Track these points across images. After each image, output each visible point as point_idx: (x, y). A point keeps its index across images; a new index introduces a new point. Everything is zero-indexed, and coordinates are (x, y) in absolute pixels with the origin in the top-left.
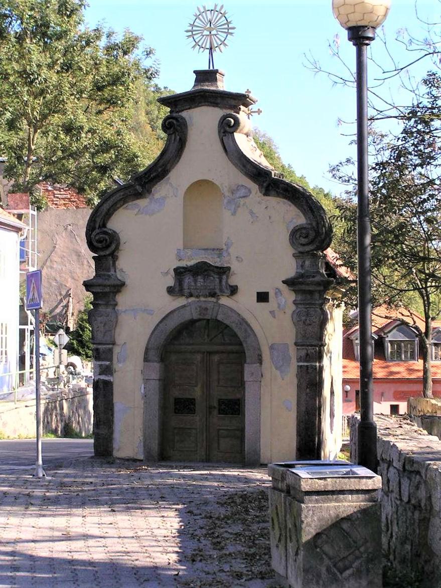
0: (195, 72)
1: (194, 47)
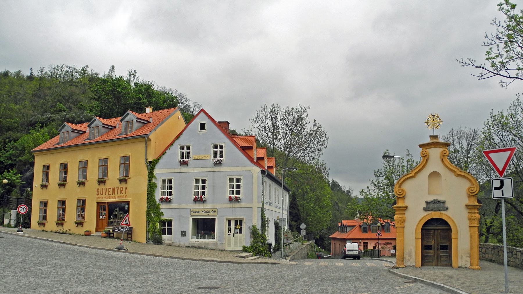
0: (430, 136)
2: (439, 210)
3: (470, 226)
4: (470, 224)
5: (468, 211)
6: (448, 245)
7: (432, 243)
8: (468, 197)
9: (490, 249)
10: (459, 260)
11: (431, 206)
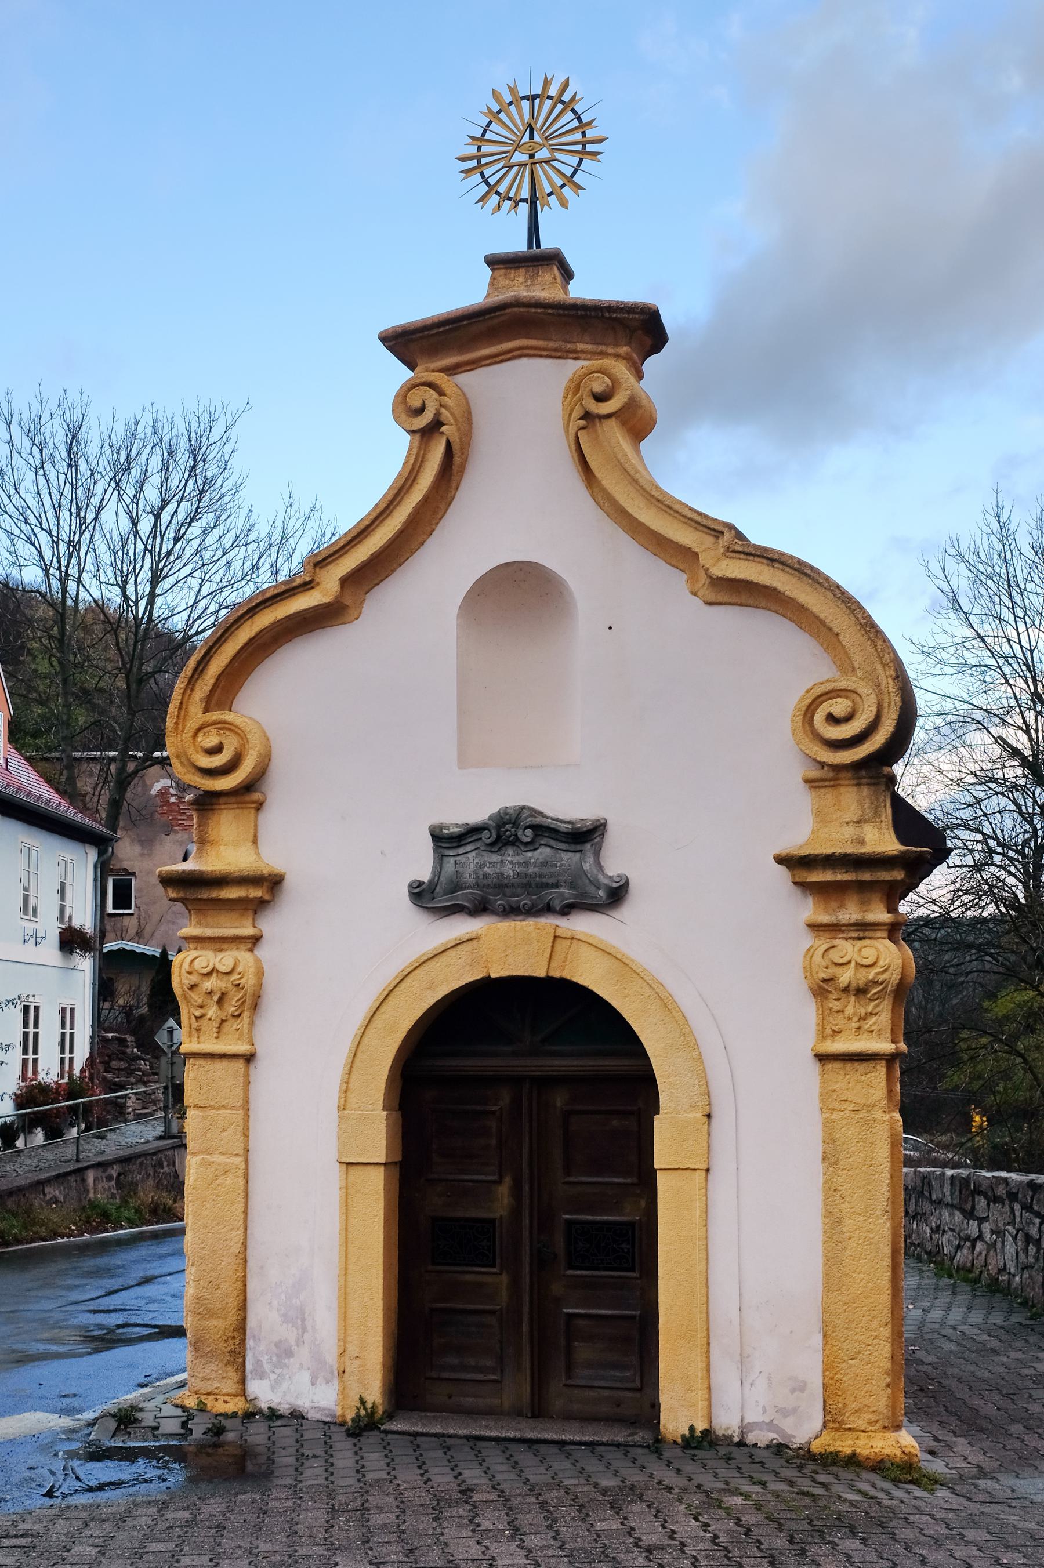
0: (494, 262)
1: (483, 199)
2: (548, 909)
3: (822, 1058)
5: (808, 909)
6: (631, 1224)
10: (725, 1374)
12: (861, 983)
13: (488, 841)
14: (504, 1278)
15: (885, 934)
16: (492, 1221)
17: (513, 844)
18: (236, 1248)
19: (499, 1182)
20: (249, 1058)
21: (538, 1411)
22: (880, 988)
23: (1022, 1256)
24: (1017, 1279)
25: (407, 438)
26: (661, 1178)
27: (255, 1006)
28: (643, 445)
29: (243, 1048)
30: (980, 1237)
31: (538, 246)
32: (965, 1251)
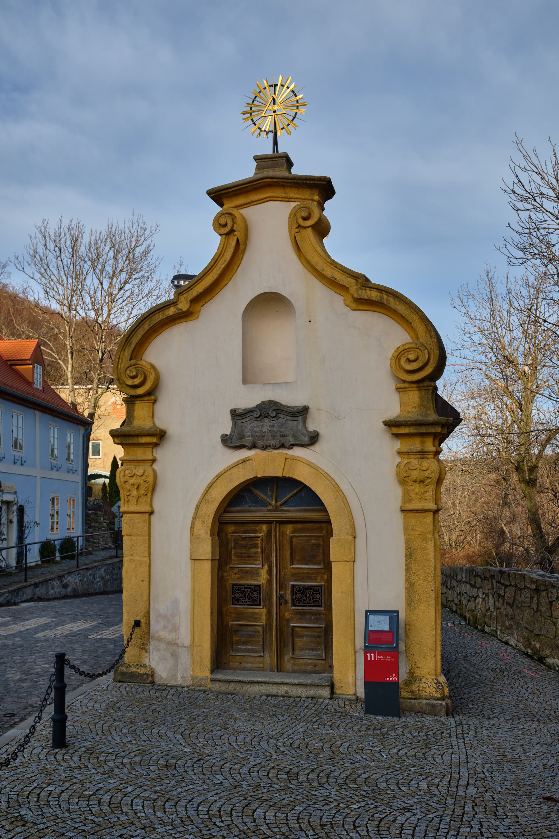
0: (256, 158)
2: (282, 446)
4: (407, 498)
5: (397, 445)
6: (321, 586)
7: (262, 579)
8: (398, 389)
9: (526, 593)
11: (249, 425)
12: (422, 478)
13: (256, 416)
14: (265, 610)
15: (432, 456)
16: (259, 586)
17: (267, 417)
18: (145, 598)
19: (262, 568)
20: (151, 513)
21: (280, 669)
22: (430, 480)
23: (497, 603)
24: (495, 614)
25: (219, 237)
26: (333, 565)
27: (153, 490)
28: (326, 241)
29: (148, 509)
30: (478, 596)
31: (277, 152)
32: (472, 602)
